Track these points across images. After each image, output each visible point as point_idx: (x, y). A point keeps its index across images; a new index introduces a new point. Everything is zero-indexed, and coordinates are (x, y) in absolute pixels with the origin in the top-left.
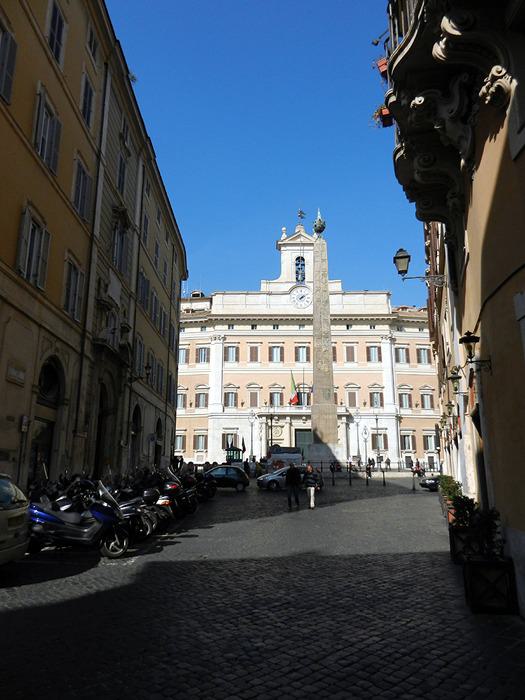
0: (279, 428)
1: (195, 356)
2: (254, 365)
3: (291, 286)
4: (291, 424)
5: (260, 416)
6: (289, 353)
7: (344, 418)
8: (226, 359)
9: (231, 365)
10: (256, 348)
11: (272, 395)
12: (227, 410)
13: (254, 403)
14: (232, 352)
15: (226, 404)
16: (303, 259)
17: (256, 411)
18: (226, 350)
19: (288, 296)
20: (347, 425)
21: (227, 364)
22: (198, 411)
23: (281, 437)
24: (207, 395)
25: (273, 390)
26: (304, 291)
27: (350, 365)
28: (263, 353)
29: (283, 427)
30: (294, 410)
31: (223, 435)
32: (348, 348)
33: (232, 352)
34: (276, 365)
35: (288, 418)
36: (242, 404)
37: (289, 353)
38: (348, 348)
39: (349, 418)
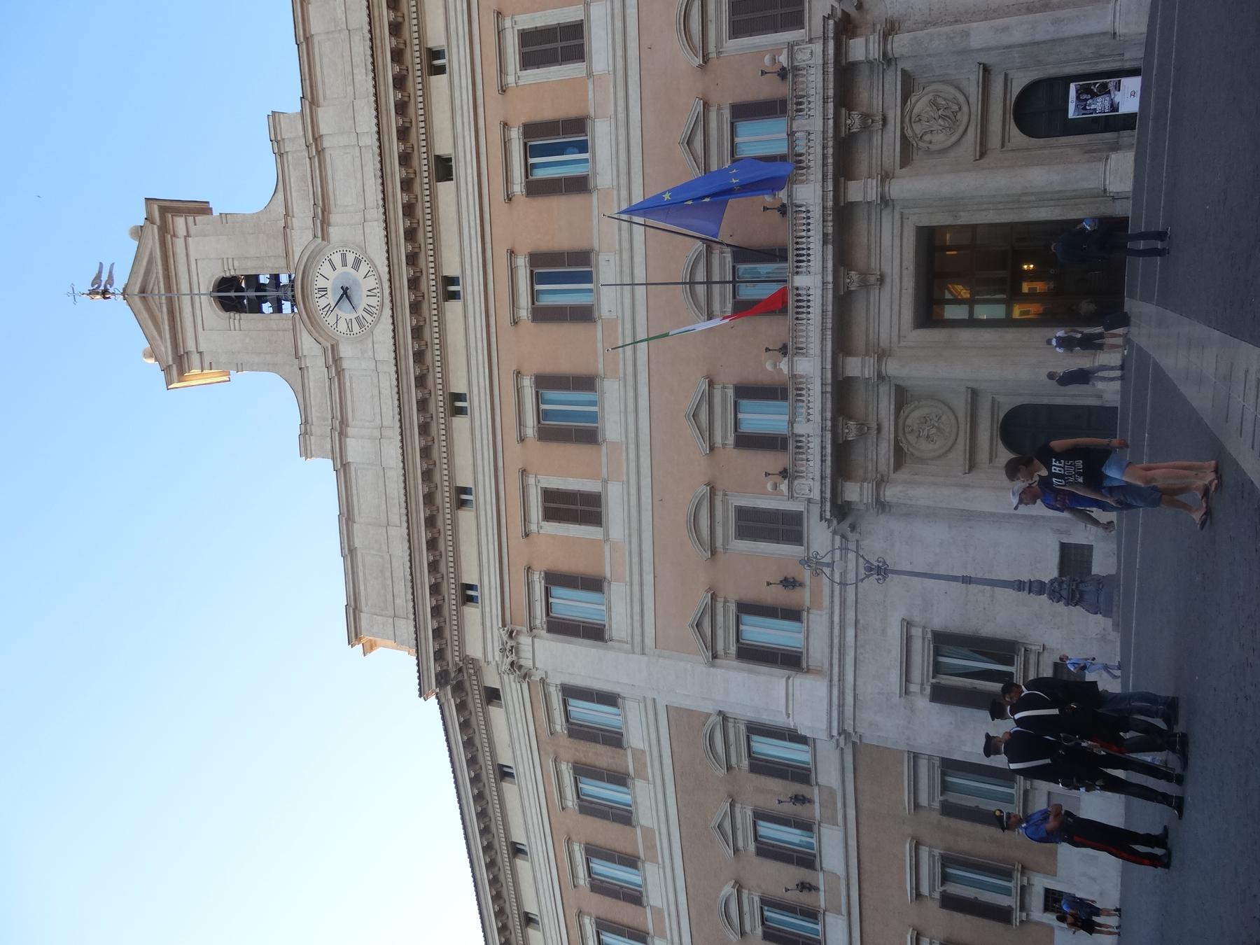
0: (914, 417)
1: (600, 748)
2: (614, 510)
3: (308, 344)
4: (882, 355)
5: (841, 511)
6: (559, 348)
7: (860, 49)
8: (594, 633)
9: (616, 608)
10: (550, 496)
11: (747, 441)
12: (818, 652)
13: (783, 527)
14: (571, 604)
15: (790, 661)
16: (226, 284)
17: (820, 536)
18: (561, 627)
19: (345, 351)
20: (891, 28)
21: (619, 625)
22: (829, 774)
23: (961, 405)
24: (755, 729)
25: (724, 435)
26: (327, 277)
27: (599, 41)
28: (567, 471)
29: (902, 397)
30: (814, 330)
31: (941, 695)
32: (528, 61)
33: (571, 604)
34: (617, 410)
35: (855, 367)
36: (790, 583)
37: (559, 348)
38: (528, 61)
39: (845, 27)
